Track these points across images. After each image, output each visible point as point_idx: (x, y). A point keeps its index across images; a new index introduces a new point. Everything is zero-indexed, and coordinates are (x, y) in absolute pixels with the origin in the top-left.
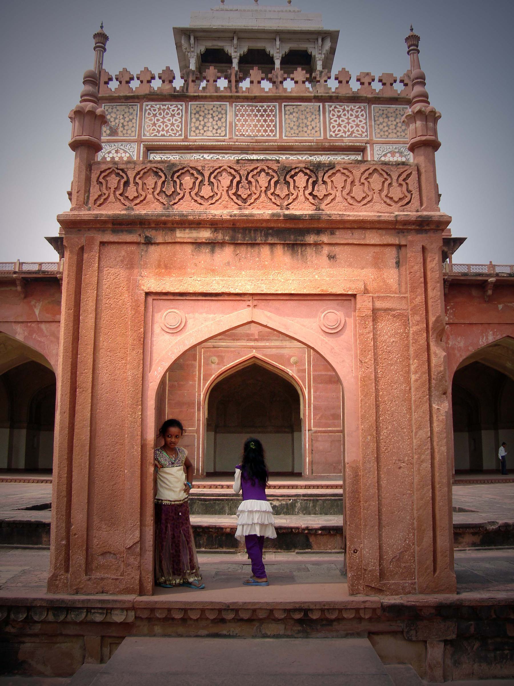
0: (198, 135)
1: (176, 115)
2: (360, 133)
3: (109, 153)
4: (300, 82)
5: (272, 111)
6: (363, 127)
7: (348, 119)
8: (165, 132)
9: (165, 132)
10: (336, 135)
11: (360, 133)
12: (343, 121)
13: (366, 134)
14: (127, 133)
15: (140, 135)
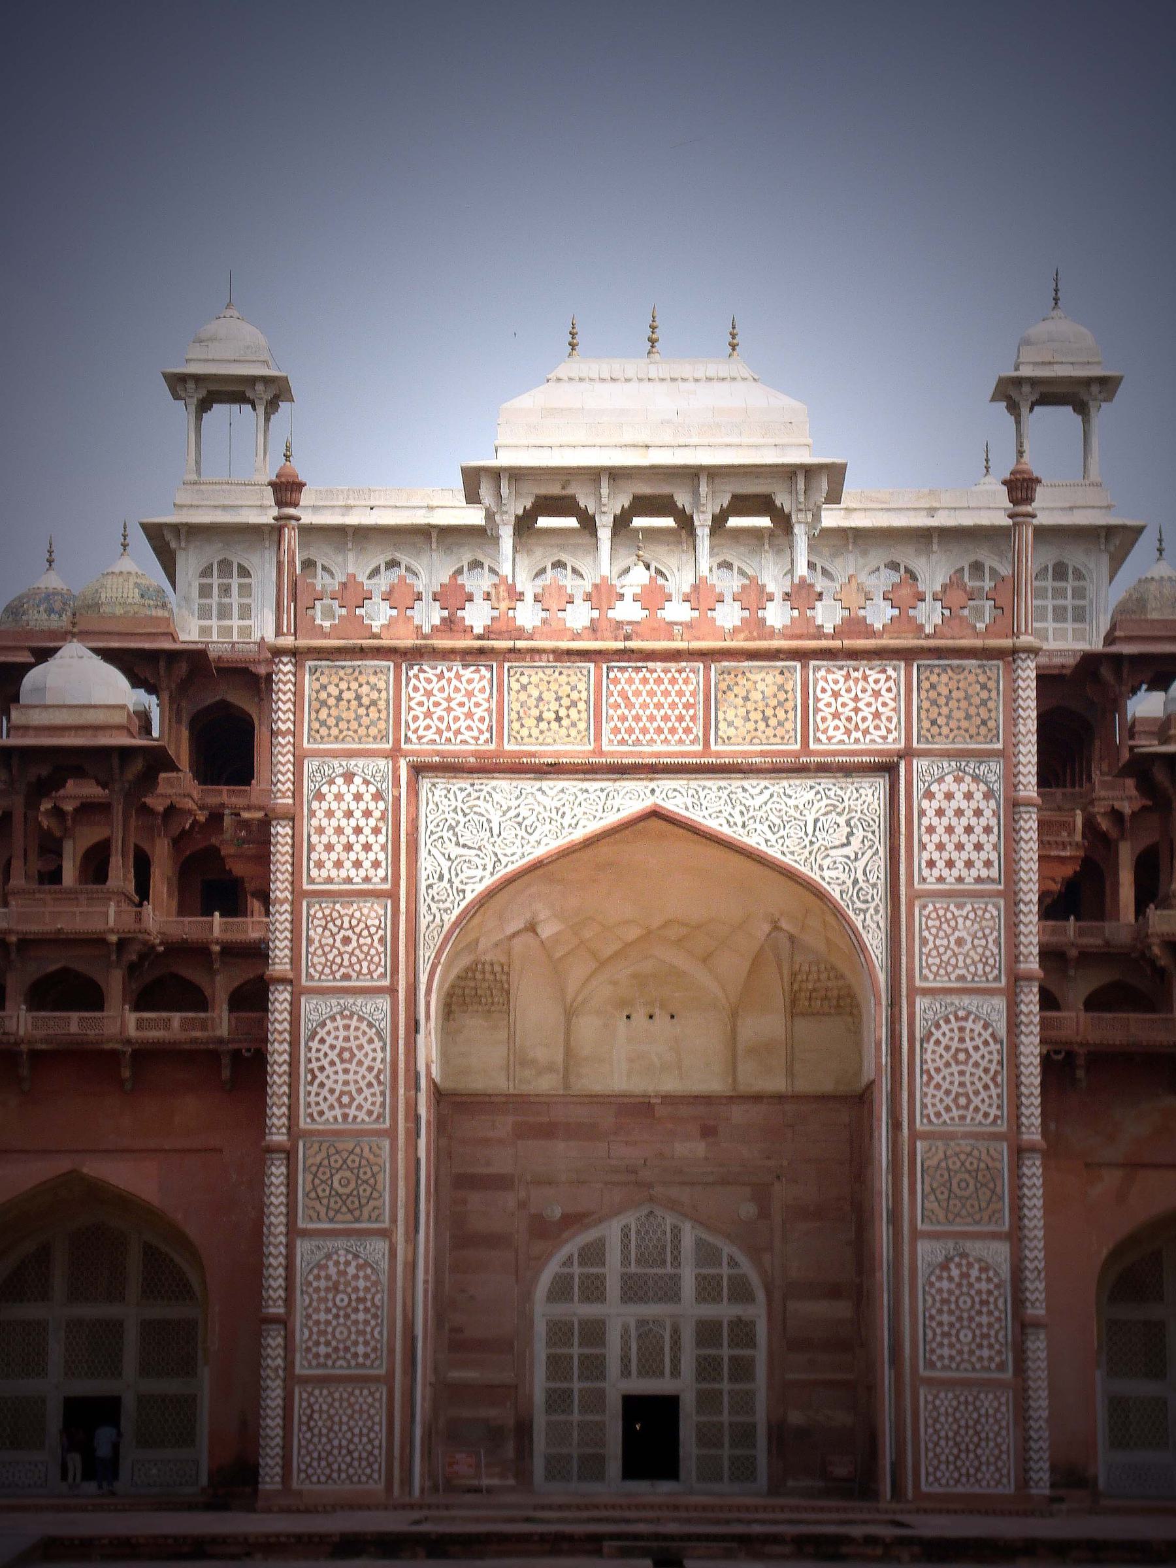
0: (526, 740)
1: (476, 692)
2: (884, 732)
3: (332, 782)
4: (754, 608)
5: (686, 681)
6: (889, 719)
7: (856, 699)
8: (451, 735)
9: (451, 735)
10: (829, 739)
11: (884, 732)
12: (844, 705)
13: (895, 734)
14: (368, 735)
15: (397, 741)
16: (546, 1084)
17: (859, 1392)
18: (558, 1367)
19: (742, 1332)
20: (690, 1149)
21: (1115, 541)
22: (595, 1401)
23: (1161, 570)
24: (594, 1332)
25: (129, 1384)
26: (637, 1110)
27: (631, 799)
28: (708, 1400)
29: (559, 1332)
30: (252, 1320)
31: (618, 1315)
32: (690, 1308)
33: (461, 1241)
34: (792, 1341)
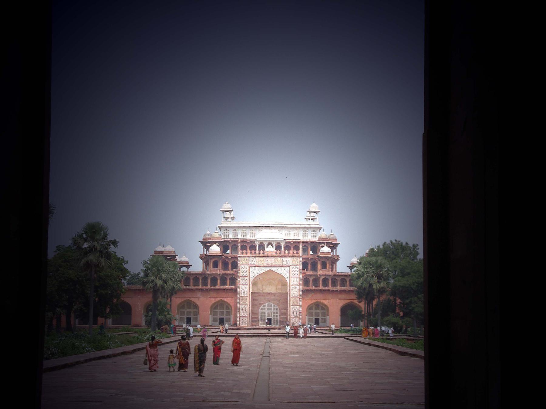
16: (260, 292)
17: (286, 318)
18: (261, 316)
19: (277, 312)
20: (273, 297)
21: (320, 228)
22: (265, 318)
23: (323, 233)
24: (264, 313)
25: (225, 317)
26: (268, 294)
27: (268, 269)
28: (274, 318)
29: (262, 313)
30: (237, 312)
31: (267, 311)
32: (273, 311)
33: (253, 305)
34: (281, 314)
